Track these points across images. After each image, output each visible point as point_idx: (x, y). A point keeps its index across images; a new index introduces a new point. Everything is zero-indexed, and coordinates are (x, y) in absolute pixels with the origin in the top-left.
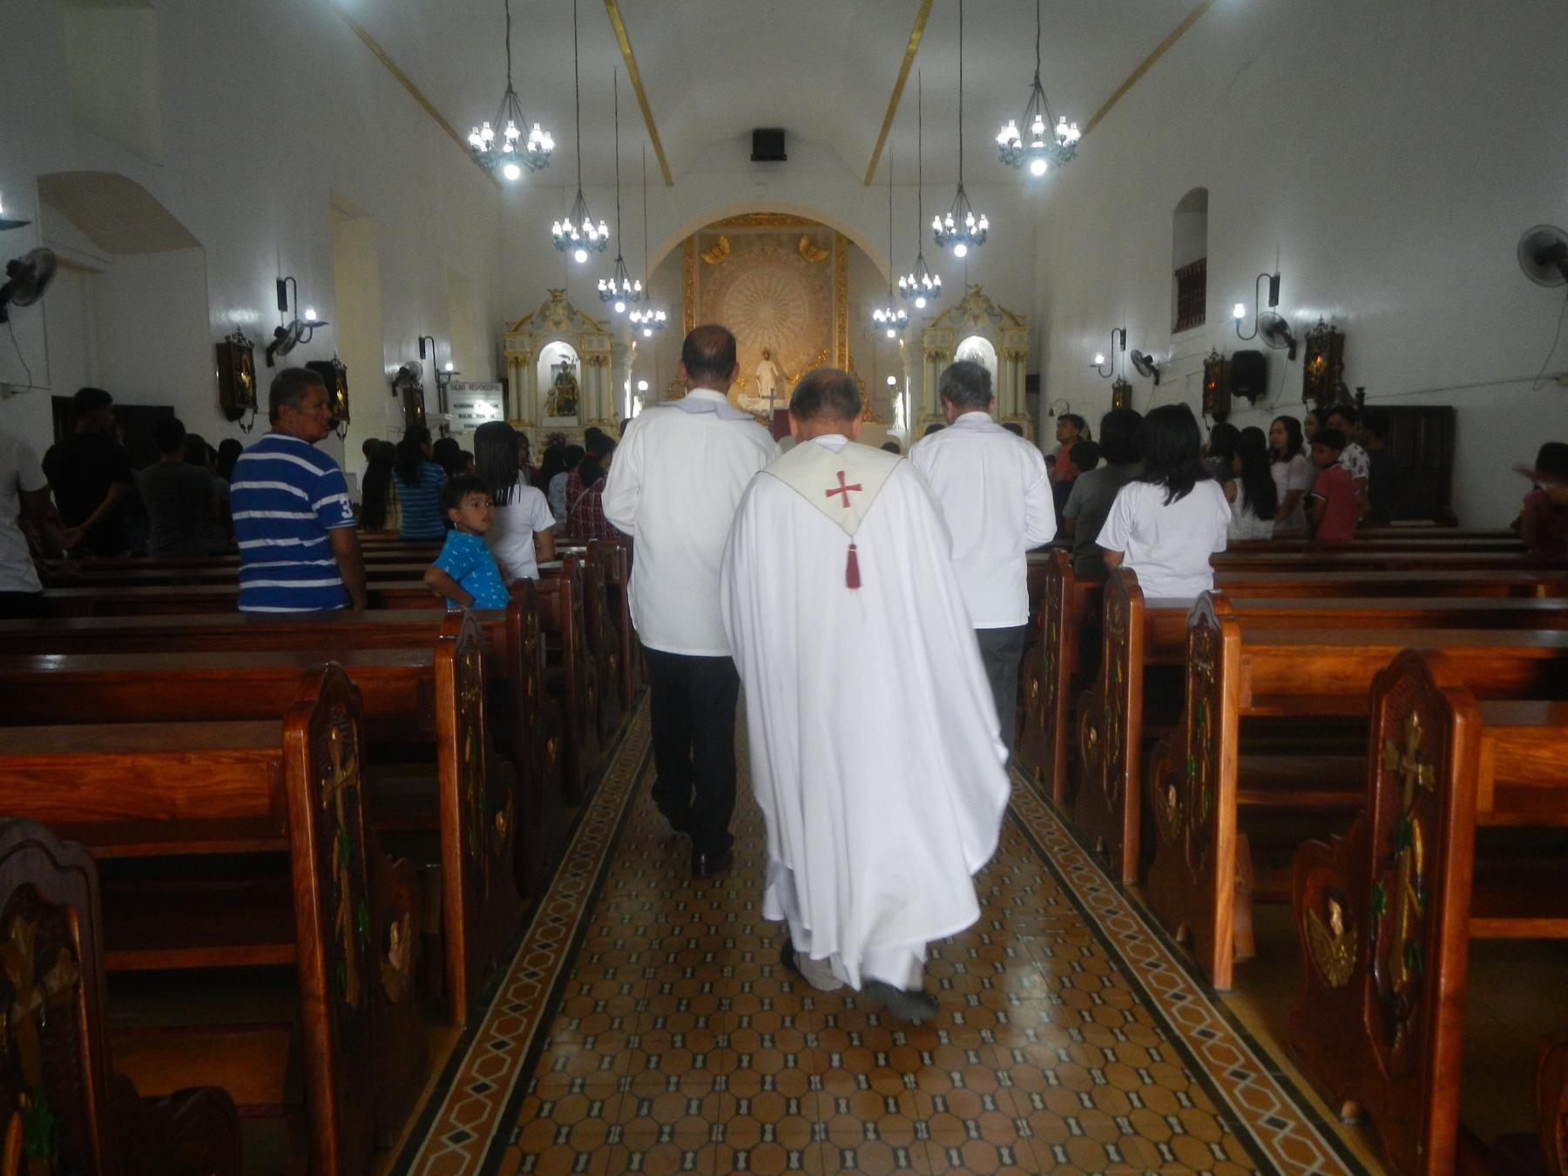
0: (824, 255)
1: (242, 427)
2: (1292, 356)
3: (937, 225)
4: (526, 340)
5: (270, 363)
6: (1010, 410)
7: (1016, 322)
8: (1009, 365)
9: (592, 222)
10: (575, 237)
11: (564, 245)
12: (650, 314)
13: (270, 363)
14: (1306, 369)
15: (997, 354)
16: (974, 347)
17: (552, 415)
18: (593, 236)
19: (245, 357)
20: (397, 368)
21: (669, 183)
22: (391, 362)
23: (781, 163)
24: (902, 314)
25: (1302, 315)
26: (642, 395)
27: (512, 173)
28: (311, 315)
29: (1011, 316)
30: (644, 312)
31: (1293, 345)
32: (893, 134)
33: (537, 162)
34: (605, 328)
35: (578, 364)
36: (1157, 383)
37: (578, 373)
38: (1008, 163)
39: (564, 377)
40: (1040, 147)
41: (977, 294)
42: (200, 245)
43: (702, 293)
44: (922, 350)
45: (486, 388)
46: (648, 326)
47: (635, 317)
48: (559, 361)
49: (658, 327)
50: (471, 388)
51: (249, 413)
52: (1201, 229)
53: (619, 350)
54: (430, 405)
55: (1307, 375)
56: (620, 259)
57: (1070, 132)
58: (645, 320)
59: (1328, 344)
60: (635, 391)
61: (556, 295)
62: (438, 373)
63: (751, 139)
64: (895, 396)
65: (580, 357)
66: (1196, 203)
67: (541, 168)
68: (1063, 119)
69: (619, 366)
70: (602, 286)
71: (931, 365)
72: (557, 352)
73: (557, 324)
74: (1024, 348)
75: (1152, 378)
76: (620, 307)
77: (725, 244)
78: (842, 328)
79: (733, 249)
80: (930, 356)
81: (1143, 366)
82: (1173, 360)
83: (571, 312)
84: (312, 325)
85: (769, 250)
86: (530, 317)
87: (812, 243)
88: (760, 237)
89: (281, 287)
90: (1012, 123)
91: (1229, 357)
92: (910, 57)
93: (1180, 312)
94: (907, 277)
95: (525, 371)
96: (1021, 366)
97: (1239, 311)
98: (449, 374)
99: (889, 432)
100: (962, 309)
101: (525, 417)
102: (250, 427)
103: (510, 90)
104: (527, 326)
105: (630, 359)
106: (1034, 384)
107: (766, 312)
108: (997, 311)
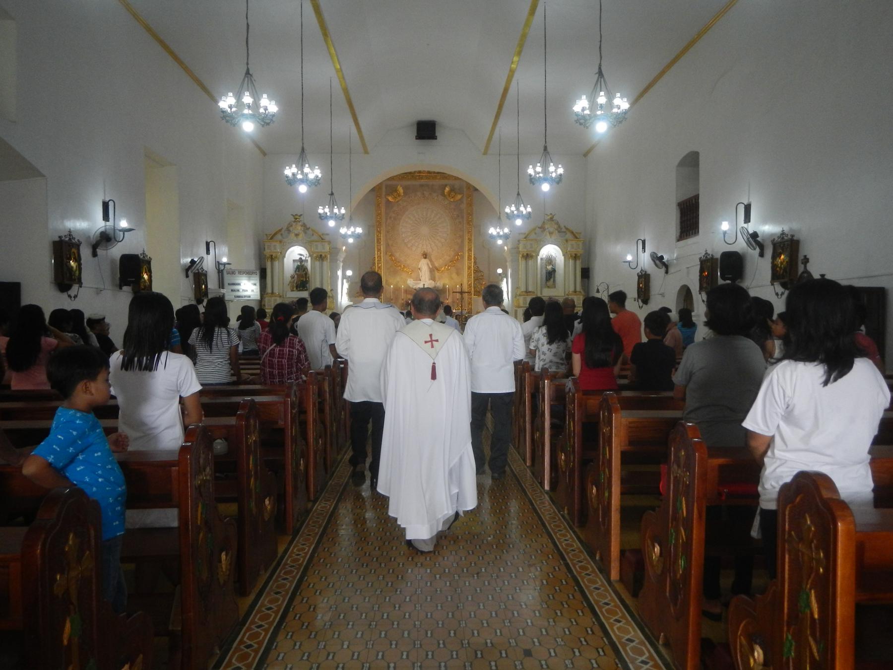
0: (459, 197)
1: (70, 296)
2: (762, 255)
3: (531, 171)
4: (278, 245)
5: (95, 254)
6: (572, 289)
7: (575, 236)
8: (571, 262)
9: (310, 167)
10: (299, 176)
11: (292, 182)
12: (352, 229)
13: (95, 254)
14: (773, 263)
15: (564, 255)
16: (551, 251)
17: (292, 291)
18: (311, 176)
19: (74, 250)
20: (189, 260)
21: (366, 152)
22: (185, 256)
23: (434, 141)
24: (506, 230)
25: (768, 229)
26: (349, 279)
27: (248, 127)
28: (124, 224)
29: (572, 233)
30: (348, 228)
31: (761, 246)
32: (501, 122)
33: (265, 121)
34: (327, 238)
35: (309, 259)
36: (667, 272)
37: (309, 265)
38: (581, 124)
39: (301, 268)
40: (602, 112)
41: (552, 219)
42: (44, 176)
44: (518, 252)
45: (249, 273)
46: (352, 236)
47: (343, 231)
48: (298, 258)
49: (357, 237)
50: (240, 273)
51: (75, 287)
52: (694, 176)
53: (335, 251)
54: (212, 284)
55: (774, 267)
56: (332, 194)
57: (622, 104)
58: (349, 233)
59: (787, 247)
60: (344, 276)
61: (296, 218)
62: (218, 264)
63: (415, 127)
64: (502, 280)
65: (310, 256)
66: (691, 161)
67: (268, 124)
68: (618, 95)
69: (334, 260)
70: (320, 211)
71: (524, 262)
72: (296, 252)
73: (297, 235)
74: (580, 251)
75: (663, 270)
76: (332, 223)
77: (401, 190)
78: (470, 240)
80: (523, 256)
81: (658, 262)
82: (677, 259)
83: (306, 228)
84: (125, 231)
85: (426, 194)
86: (280, 230)
87: (452, 190)
88: (422, 186)
89: (106, 206)
90: (584, 97)
91: (718, 256)
92: (512, 73)
93: (682, 228)
94: (510, 206)
95: (276, 263)
96: (578, 262)
97: (725, 226)
98: (225, 264)
100: (542, 228)
101: (276, 291)
102: (75, 297)
103: (248, 73)
104: (279, 237)
105: (342, 257)
106: (586, 273)
107: (425, 230)
108: (564, 230)
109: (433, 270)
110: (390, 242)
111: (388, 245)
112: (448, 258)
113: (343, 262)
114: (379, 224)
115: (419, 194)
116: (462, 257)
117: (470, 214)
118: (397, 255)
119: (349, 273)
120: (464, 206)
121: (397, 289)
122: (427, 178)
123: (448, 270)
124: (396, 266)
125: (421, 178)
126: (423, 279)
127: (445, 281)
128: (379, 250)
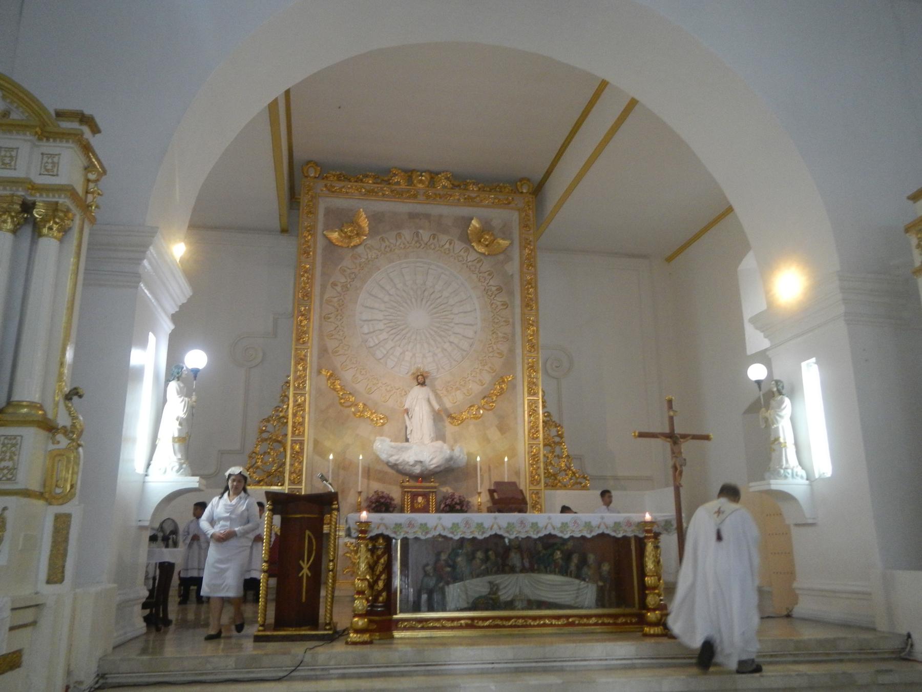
0: (504, 243)
26: (192, 383)
60: (174, 371)
77: (364, 223)
79: (374, 231)
85: (425, 235)
87: (486, 228)
88: (412, 216)
99: (777, 484)
107: (418, 318)
109: (442, 418)
110: (331, 344)
112: (476, 388)
113: (175, 318)
114: (307, 295)
115: (407, 234)
116: (514, 386)
117: (530, 285)
118: (347, 375)
119: (196, 359)
120: (513, 267)
121: (344, 465)
123: (476, 417)
124: (343, 407)
125: (415, 196)
126: (414, 438)
127: (469, 447)
128: (301, 360)
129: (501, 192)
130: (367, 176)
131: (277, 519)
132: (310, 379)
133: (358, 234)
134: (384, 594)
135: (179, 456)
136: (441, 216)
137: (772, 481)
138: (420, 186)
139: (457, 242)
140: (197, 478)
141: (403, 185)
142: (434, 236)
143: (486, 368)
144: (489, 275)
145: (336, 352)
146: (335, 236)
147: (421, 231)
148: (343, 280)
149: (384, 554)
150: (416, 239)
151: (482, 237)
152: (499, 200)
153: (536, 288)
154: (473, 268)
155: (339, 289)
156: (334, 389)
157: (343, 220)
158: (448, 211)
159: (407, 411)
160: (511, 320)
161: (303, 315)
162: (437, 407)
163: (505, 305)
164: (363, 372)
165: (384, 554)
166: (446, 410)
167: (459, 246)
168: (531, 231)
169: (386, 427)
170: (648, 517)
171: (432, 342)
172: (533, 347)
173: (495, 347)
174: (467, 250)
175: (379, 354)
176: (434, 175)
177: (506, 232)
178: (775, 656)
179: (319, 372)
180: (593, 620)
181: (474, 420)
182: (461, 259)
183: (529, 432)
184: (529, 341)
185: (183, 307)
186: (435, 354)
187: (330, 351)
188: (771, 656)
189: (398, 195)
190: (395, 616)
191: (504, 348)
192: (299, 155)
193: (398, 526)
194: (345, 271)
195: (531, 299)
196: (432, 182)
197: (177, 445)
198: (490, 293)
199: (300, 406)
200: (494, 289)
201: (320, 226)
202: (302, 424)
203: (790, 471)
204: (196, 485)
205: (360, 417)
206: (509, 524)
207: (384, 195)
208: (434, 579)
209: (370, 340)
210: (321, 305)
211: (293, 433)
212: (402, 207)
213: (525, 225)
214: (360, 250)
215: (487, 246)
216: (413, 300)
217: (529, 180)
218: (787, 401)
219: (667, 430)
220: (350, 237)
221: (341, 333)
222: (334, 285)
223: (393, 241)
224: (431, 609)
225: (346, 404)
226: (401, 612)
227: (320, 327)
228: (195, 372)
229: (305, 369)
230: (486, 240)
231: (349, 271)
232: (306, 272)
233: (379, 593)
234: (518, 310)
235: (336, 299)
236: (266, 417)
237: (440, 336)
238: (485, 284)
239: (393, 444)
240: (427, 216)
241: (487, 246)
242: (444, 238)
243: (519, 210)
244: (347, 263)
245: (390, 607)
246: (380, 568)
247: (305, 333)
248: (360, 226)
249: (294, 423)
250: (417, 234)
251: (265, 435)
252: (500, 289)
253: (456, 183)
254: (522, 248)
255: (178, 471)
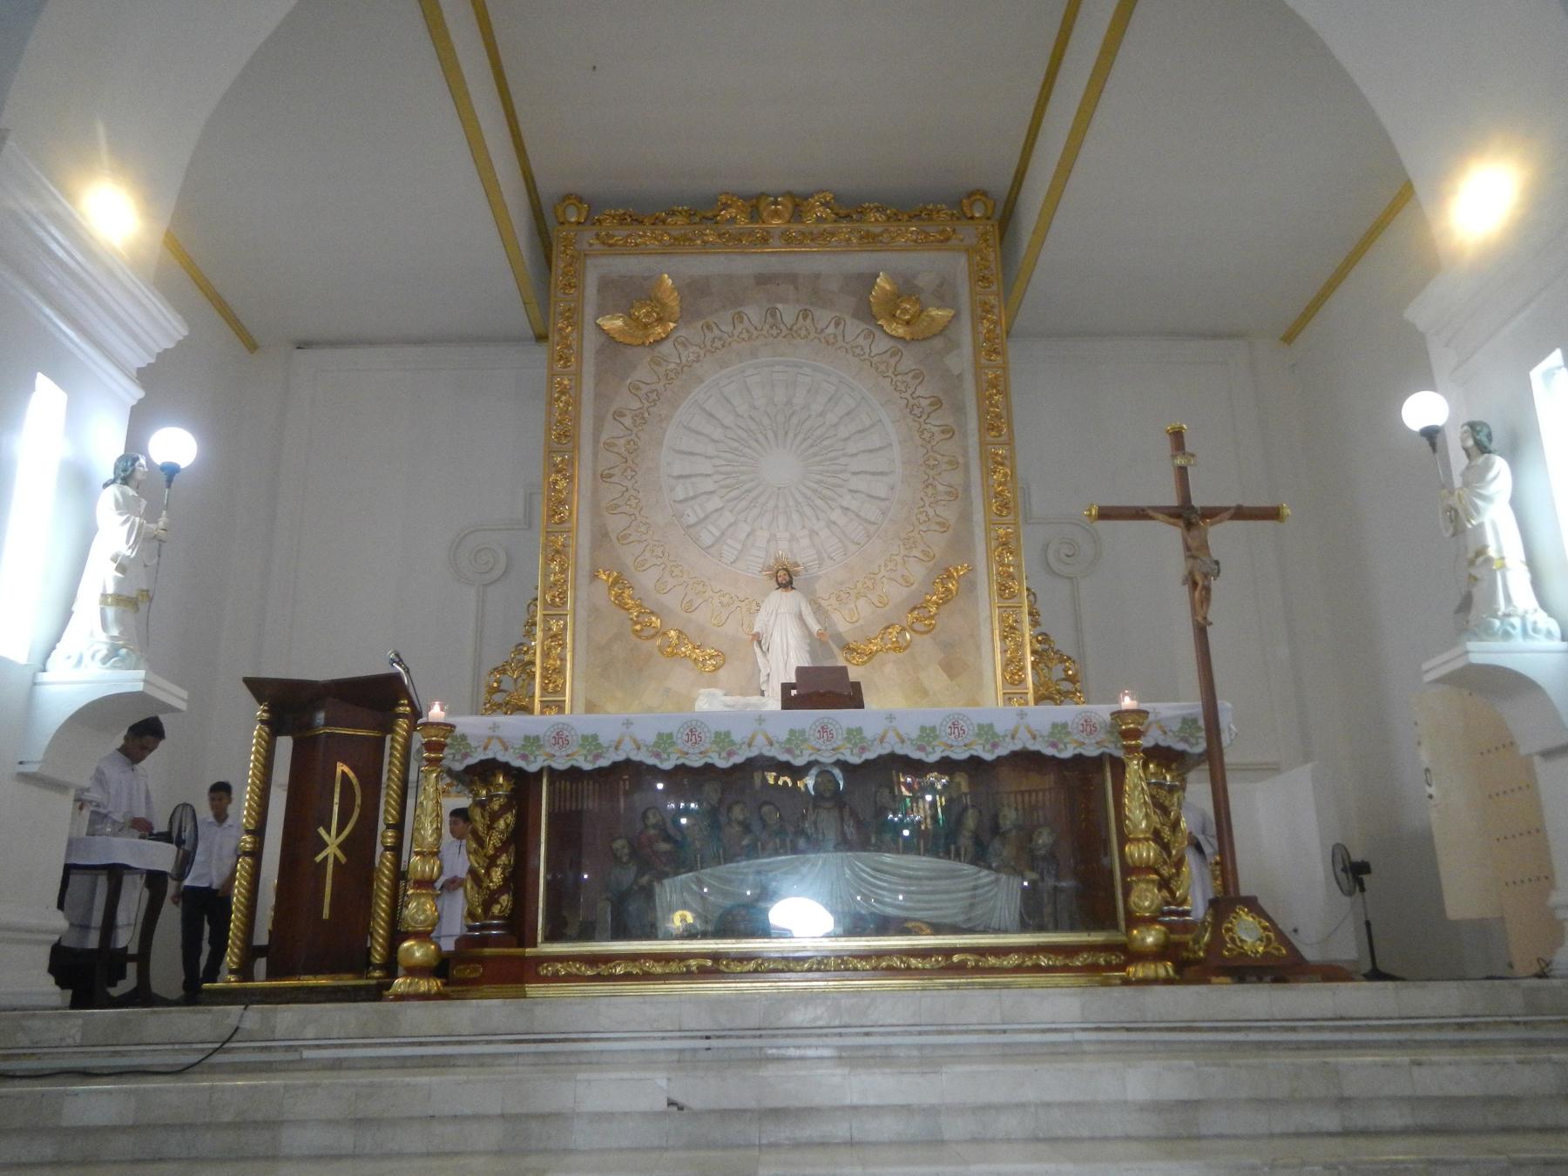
0: (939, 313)
43: (599, 421)
77: (673, 301)
85: (788, 312)
87: (906, 289)
88: (763, 280)
99: (1482, 652)
107: (781, 466)
110: (616, 524)
111: (601, 537)
112: (896, 593)
113: (144, 377)
115: (753, 313)
116: (972, 587)
117: (995, 388)
118: (647, 580)
119: (175, 446)
120: (962, 360)
122: (788, 240)
123: (898, 648)
125: (765, 241)
129: (931, 219)
130: (673, 213)
131: (285, 745)
132: (575, 588)
133: (660, 320)
134: (505, 899)
135: (115, 632)
136: (818, 276)
137: (1472, 645)
138: (776, 222)
139: (849, 320)
140: (141, 673)
141: (743, 222)
142: (805, 314)
143: (915, 552)
144: (915, 377)
145: (625, 537)
146: (614, 323)
147: (780, 306)
148: (635, 405)
149: (504, 809)
150: (770, 320)
151: (898, 307)
152: (927, 234)
153: (1005, 393)
154: (882, 368)
155: (628, 421)
156: (622, 606)
157: (631, 295)
158: (830, 263)
159: (758, 639)
160: (961, 460)
161: (559, 472)
162: (815, 627)
163: (948, 431)
164: (677, 571)
165: (504, 809)
166: (838, 637)
167: (854, 328)
168: (994, 288)
169: (722, 673)
170: (1127, 703)
171: (808, 511)
172: (1005, 505)
173: (931, 512)
174: (870, 335)
175: (707, 539)
176: (798, 204)
177: (943, 294)
178: (1472, 1026)
179: (594, 576)
180: (1014, 960)
181: (892, 655)
182: (858, 351)
183: (1004, 670)
184: (998, 495)
185: (163, 356)
186: (813, 533)
187: (613, 536)
188: (1461, 1027)
189: (735, 241)
190: (529, 951)
191: (949, 514)
192: (548, 187)
193: (532, 742)
194: (638, 388)
195: (999, 416)
196: (797, 214)
197: (111, 612)
198: (917, 411)
199: (557, 637)
200: (925, 403)
201: (589, 311)
202: (560, 671)
203: (1516, 621)
204: (139, 687)
205: (673, 654)
206: (792, 732)
207: (705, 243)
208: (633, 870)
209: (689, 511)
210: (595, 454)
211: (544, 689)
212: (745, 265)
213: (980, 278)
214: (666, 348)
215: (908, 323)
216: (770, 435)
217: (985, 194)
218: (1500, 465)
219: (1172, 500)
220: (646, 326)
221: (633, 502)
222: (619, 414)
223: (727, 328)
224: (620, 933)
225: (645, 634)
226: (551, 937)
227: (595, 491)
228: (171, 471)
229: (563, 571)
230: (905, 311)
231: (645, 389)
232: (562, 393)
233: (490, 900)
234: (973, 440)
235: (623, 441)
236: (499, 664)
237: (823, 498)
238: (907, 395)
239: (728, 698)
240: (792, 278)
241: (908, 323)
242: (824, 316)
243: (967, 250)
244: (642, 373)
245: (518, 927)
246: (494, 841)
247: (562, 502)
248: (664, 305)
249: (545, 669)
250: (773, 312)
251: (498, 698)
252: (937, 403)
253: (843, 212)
254: (976, 320)
255: (105, 660)
